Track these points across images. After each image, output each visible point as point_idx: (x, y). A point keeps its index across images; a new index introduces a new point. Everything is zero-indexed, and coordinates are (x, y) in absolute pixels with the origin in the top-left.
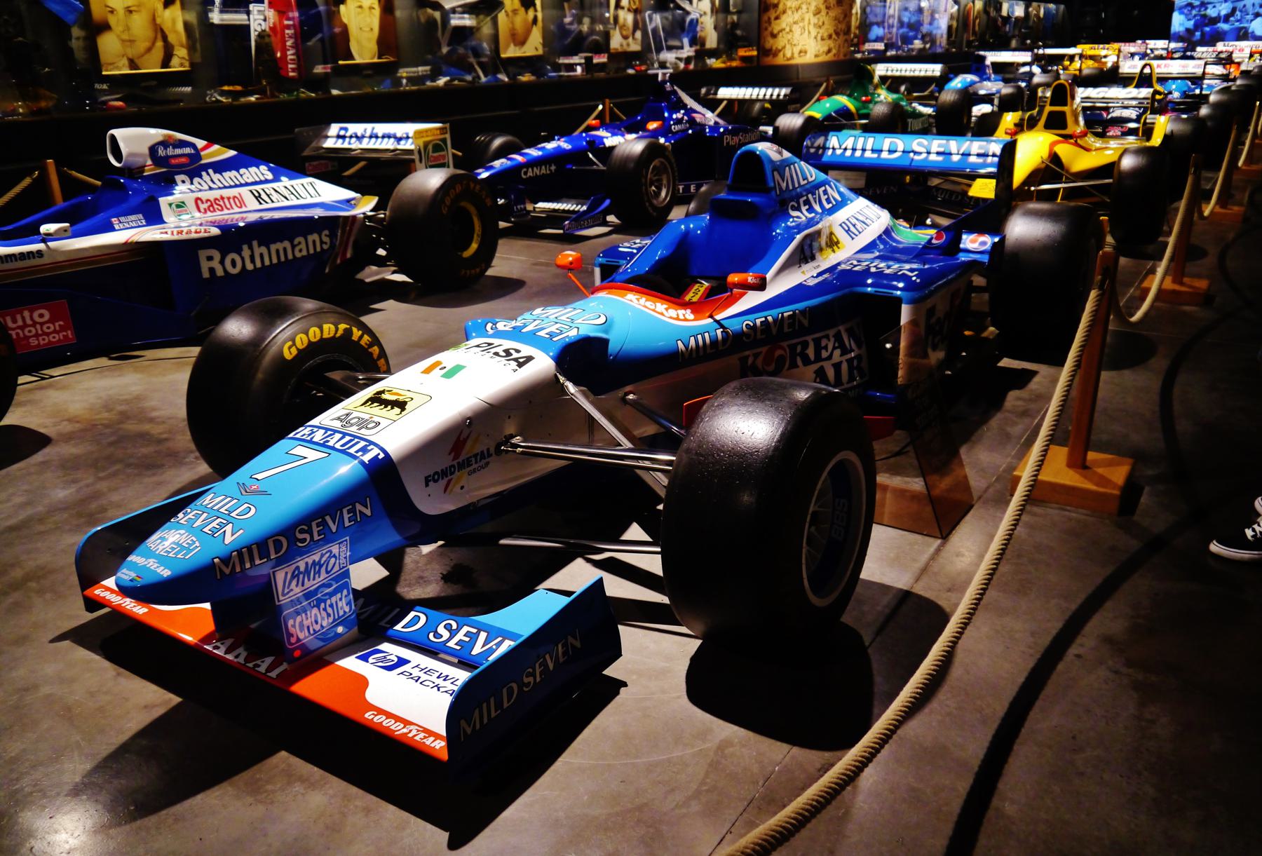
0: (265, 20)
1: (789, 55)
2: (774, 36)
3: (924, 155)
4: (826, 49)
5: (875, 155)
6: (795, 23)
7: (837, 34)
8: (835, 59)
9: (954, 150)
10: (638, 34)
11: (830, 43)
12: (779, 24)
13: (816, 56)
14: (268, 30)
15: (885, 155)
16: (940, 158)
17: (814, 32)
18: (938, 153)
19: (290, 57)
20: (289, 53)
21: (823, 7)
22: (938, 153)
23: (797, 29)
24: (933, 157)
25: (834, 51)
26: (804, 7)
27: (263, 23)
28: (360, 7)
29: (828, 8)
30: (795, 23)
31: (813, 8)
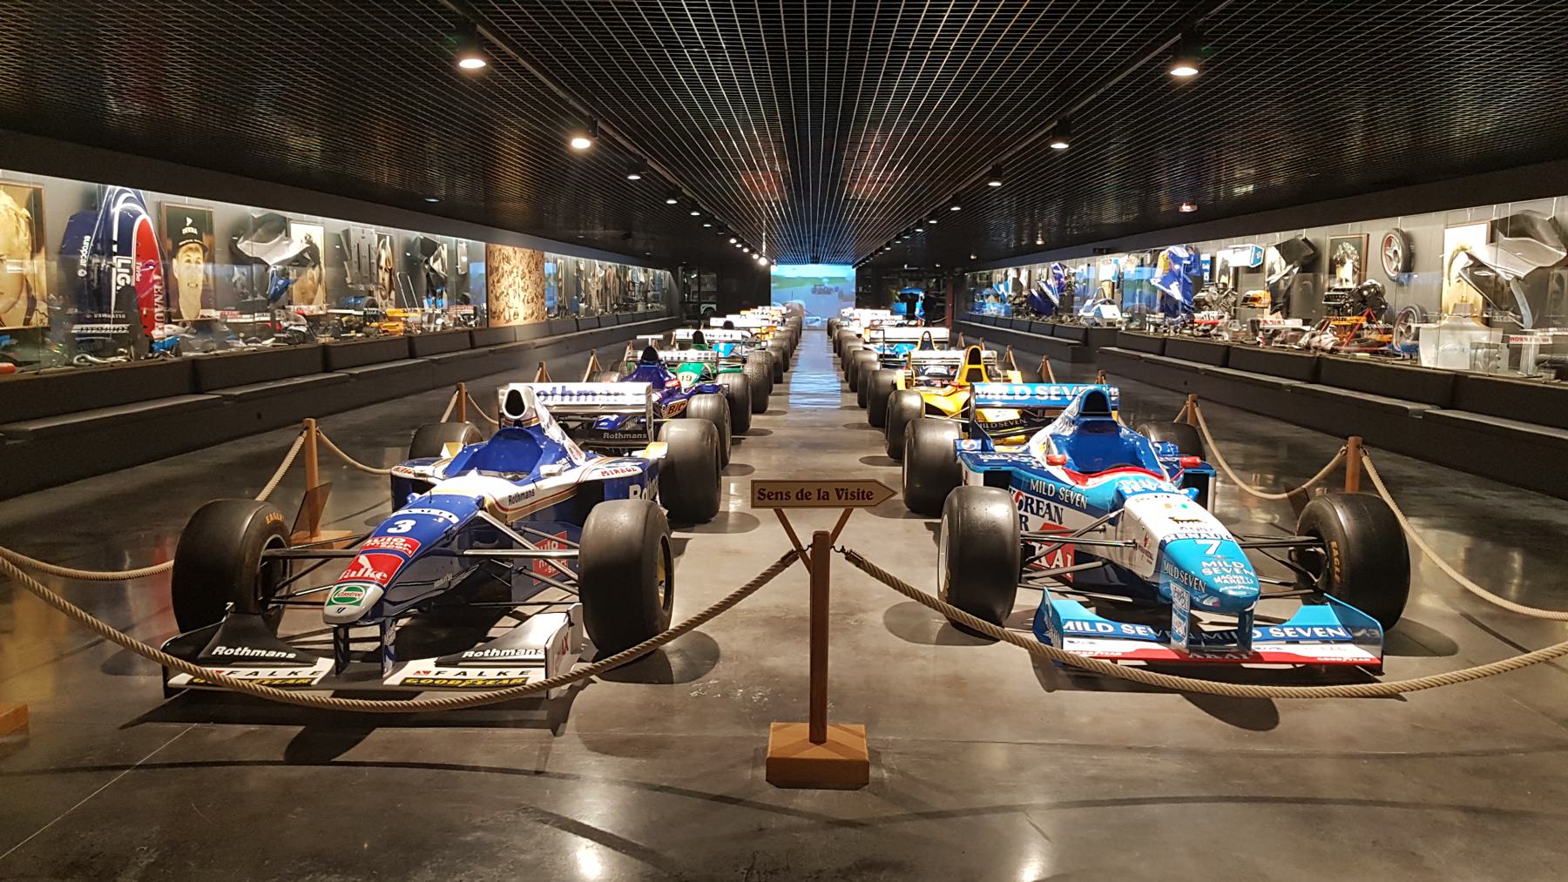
0: (130, 274)
1: (507, 318)
2: (497, 299)
3: (1046, 397)
4: (530, 312)
5: (1011, 398)
6: (510, 286)
7: (537, 297)
8: (536, 321)
9: (1067, 393)
10: (393, 293)
11: (532, 305)
12: (499, 287)
13: (525, 318)
14: (133, 284)
15: (1018, 397)
16: (1059, 398)
17: (522, 294)
18: (1056, 395)
19: (156, 315)
20: (156, 310)
21: (526, 271)
22: (1056, 395)
23: (511, 291)
24: (1053, 398)
25: (536, 314)
26: (515, 270)
27: (128, 277)
28: (189, 261)
29: (530, 272)
30: (510, 286)
31: (520, 273)
